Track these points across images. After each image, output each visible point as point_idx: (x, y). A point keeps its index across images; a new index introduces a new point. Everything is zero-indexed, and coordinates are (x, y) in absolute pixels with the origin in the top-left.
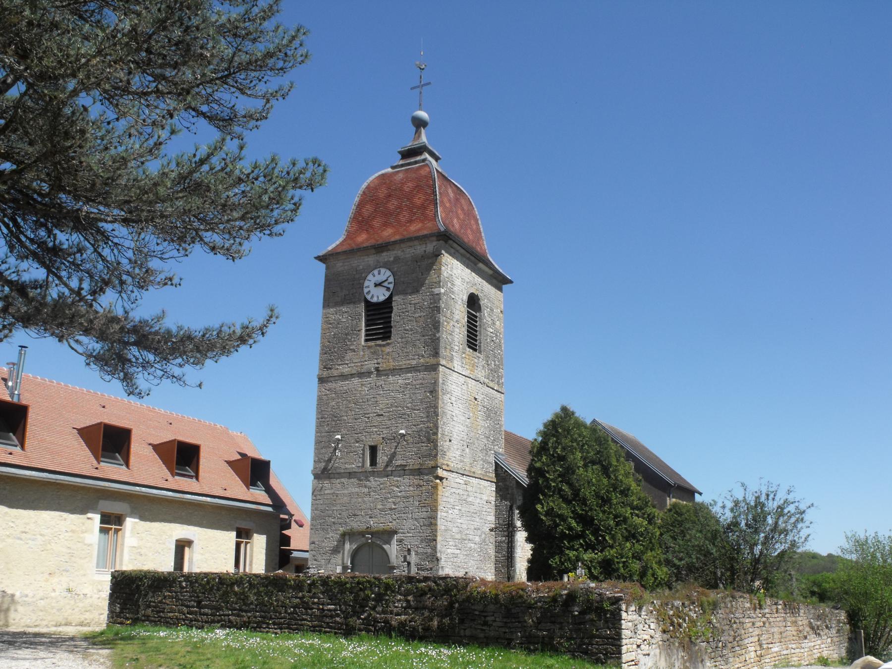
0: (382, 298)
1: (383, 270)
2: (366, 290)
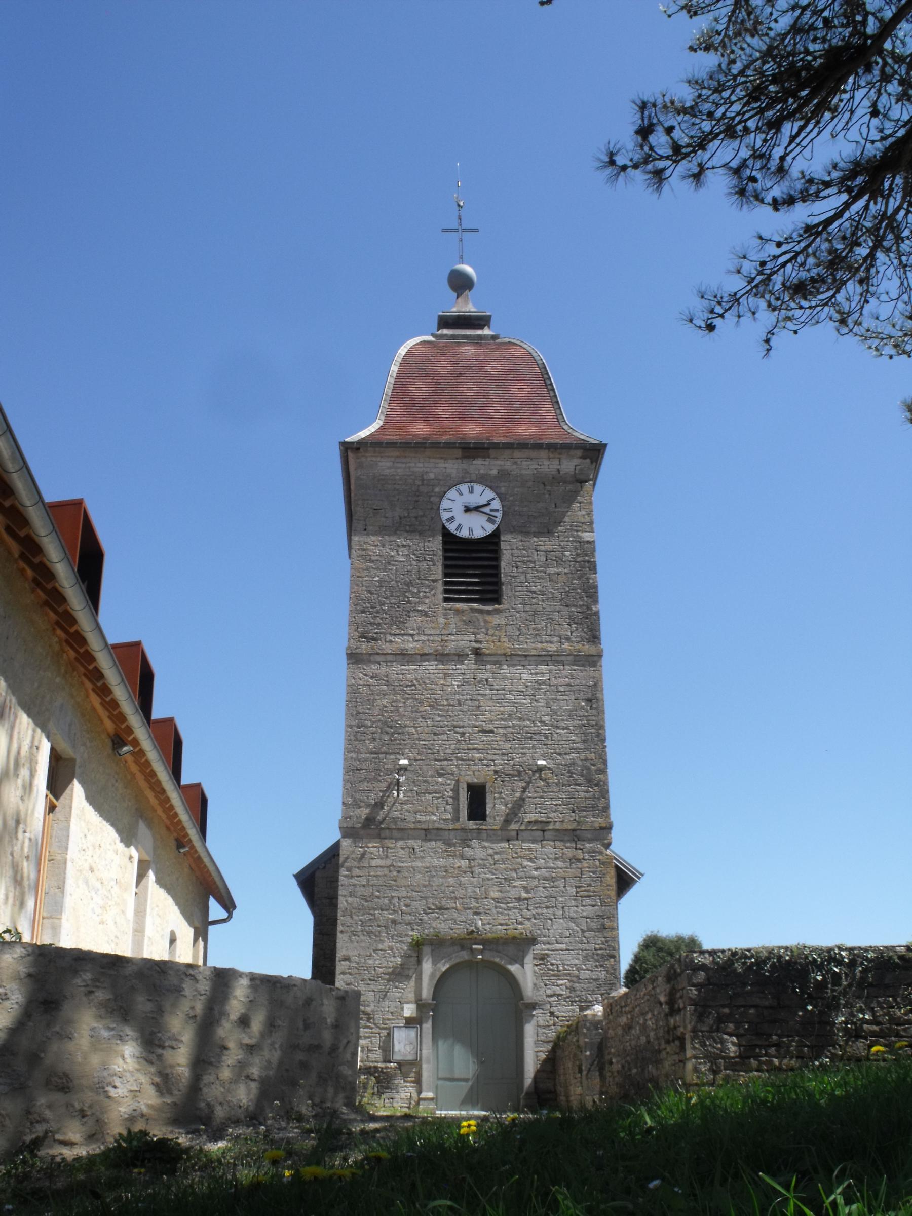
0: (479, 534)
1: (478, 488)
2: (445, 516)
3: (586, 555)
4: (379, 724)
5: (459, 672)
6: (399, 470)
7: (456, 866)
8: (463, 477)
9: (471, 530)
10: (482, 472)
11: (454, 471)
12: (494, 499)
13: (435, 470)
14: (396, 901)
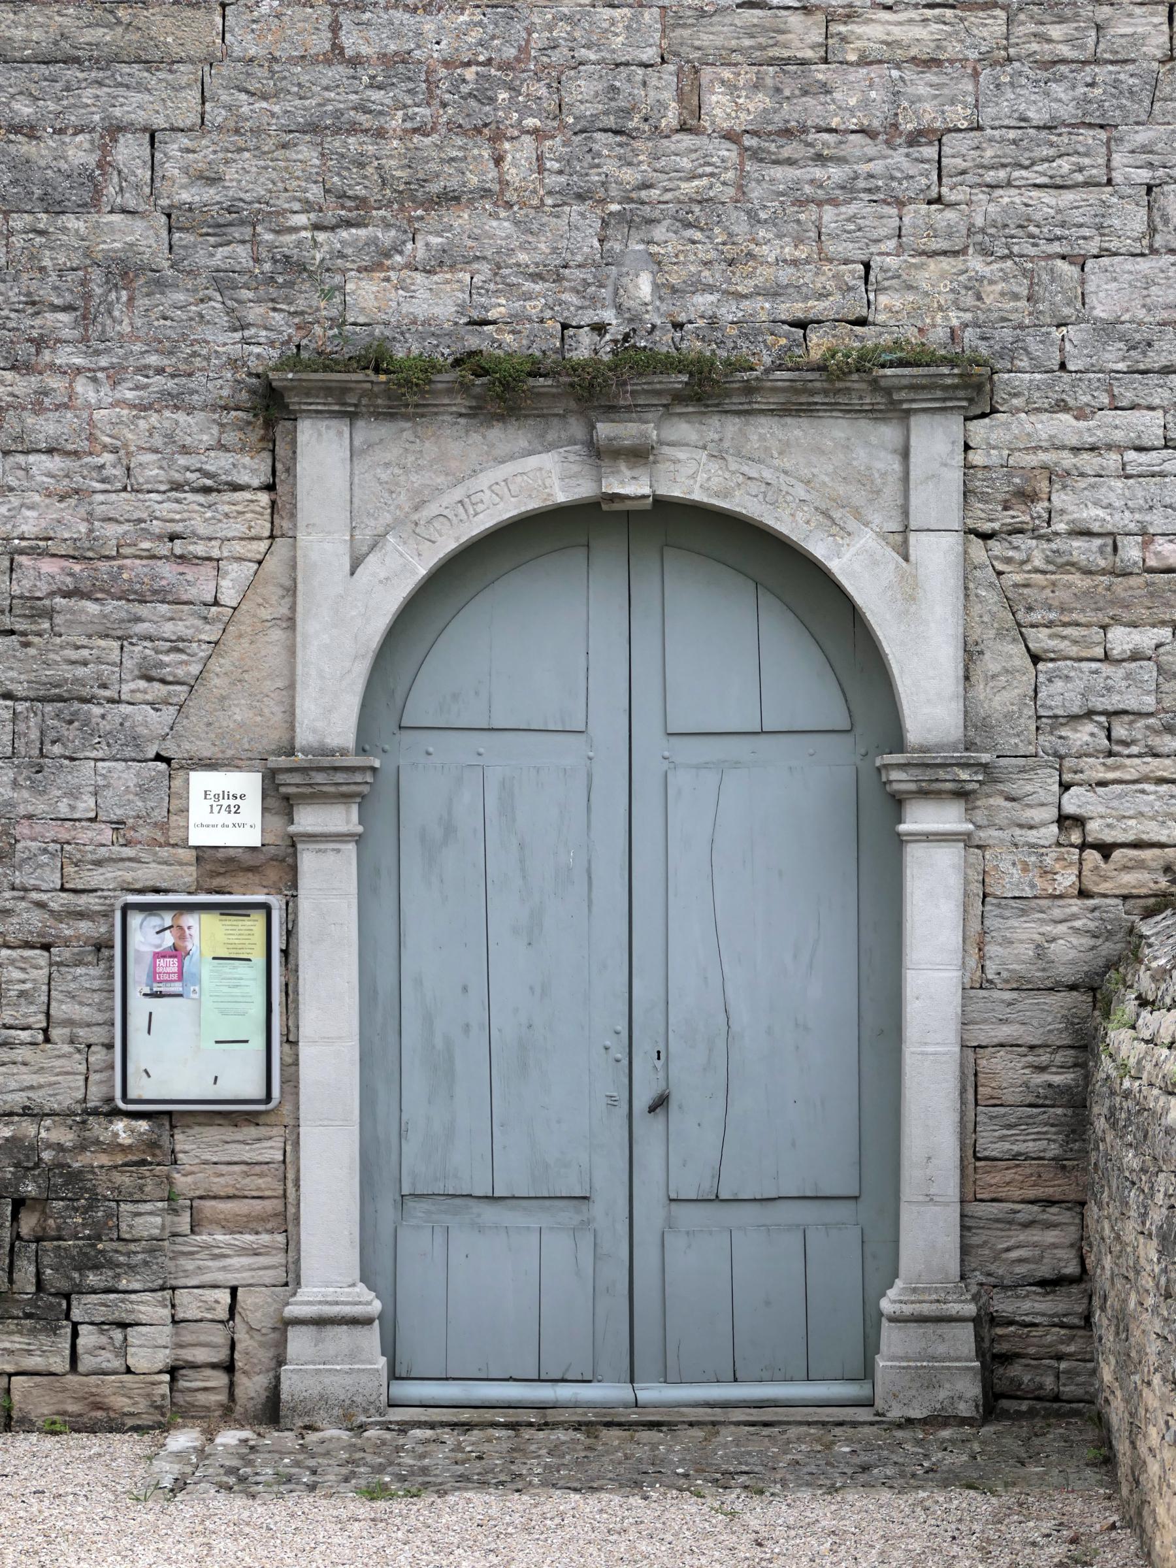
14: (129, 152)
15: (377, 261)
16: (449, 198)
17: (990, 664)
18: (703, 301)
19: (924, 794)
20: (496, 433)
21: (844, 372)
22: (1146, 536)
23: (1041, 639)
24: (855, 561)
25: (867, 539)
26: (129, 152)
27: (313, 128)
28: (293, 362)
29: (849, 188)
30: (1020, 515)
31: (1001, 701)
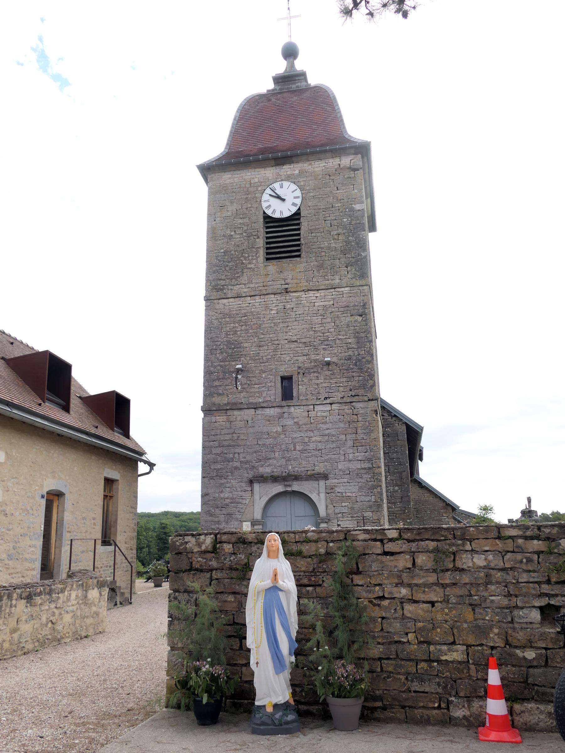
0: (287, 214)
2: (264, 205)
3: (358, 220)
4: (226, 343)
5: (274, 305)
6: (236, 179)
7: (274, 431)
8: (276, 178)
9: (281, 213)
10: (288, 173)
11: (271, 175)
12: (296, 190)
13: (258, 176)
14: (236, 455)
15: (262, 466)
16: (270, 459)
17: (329, 507)
18: (297, 469)
19: (322, 522)
20: (275, 484)
21: (311, 476)
22: (346, 493)
23: (335, 505)
24: (314, 497)
25: (315, 494)
26: (236, 455)
27: (255, 452)
28: (253, 477)
29: (312, 456)
30: (332, 491)
31: (330, 512)
